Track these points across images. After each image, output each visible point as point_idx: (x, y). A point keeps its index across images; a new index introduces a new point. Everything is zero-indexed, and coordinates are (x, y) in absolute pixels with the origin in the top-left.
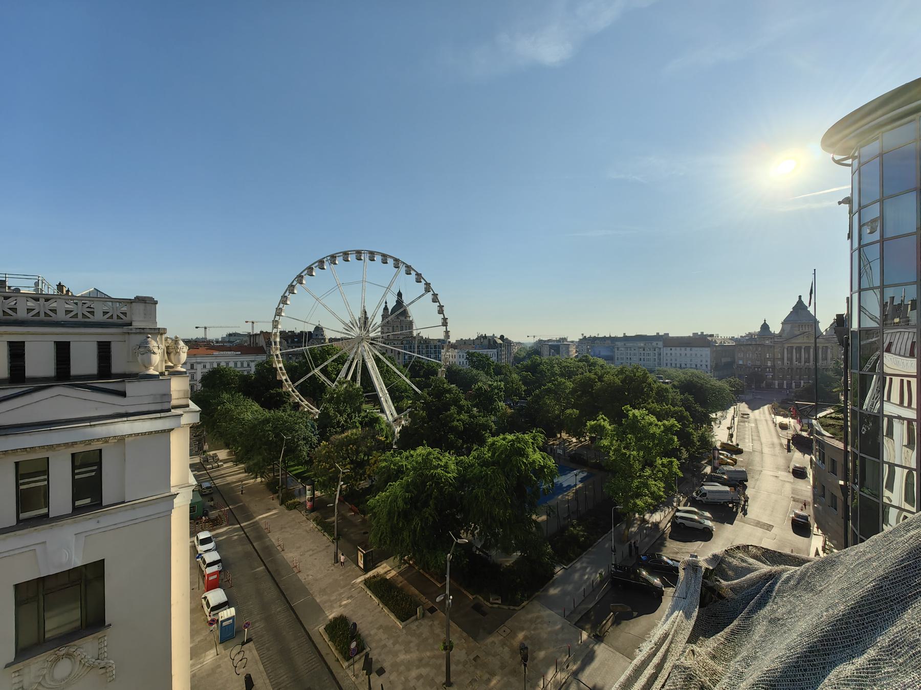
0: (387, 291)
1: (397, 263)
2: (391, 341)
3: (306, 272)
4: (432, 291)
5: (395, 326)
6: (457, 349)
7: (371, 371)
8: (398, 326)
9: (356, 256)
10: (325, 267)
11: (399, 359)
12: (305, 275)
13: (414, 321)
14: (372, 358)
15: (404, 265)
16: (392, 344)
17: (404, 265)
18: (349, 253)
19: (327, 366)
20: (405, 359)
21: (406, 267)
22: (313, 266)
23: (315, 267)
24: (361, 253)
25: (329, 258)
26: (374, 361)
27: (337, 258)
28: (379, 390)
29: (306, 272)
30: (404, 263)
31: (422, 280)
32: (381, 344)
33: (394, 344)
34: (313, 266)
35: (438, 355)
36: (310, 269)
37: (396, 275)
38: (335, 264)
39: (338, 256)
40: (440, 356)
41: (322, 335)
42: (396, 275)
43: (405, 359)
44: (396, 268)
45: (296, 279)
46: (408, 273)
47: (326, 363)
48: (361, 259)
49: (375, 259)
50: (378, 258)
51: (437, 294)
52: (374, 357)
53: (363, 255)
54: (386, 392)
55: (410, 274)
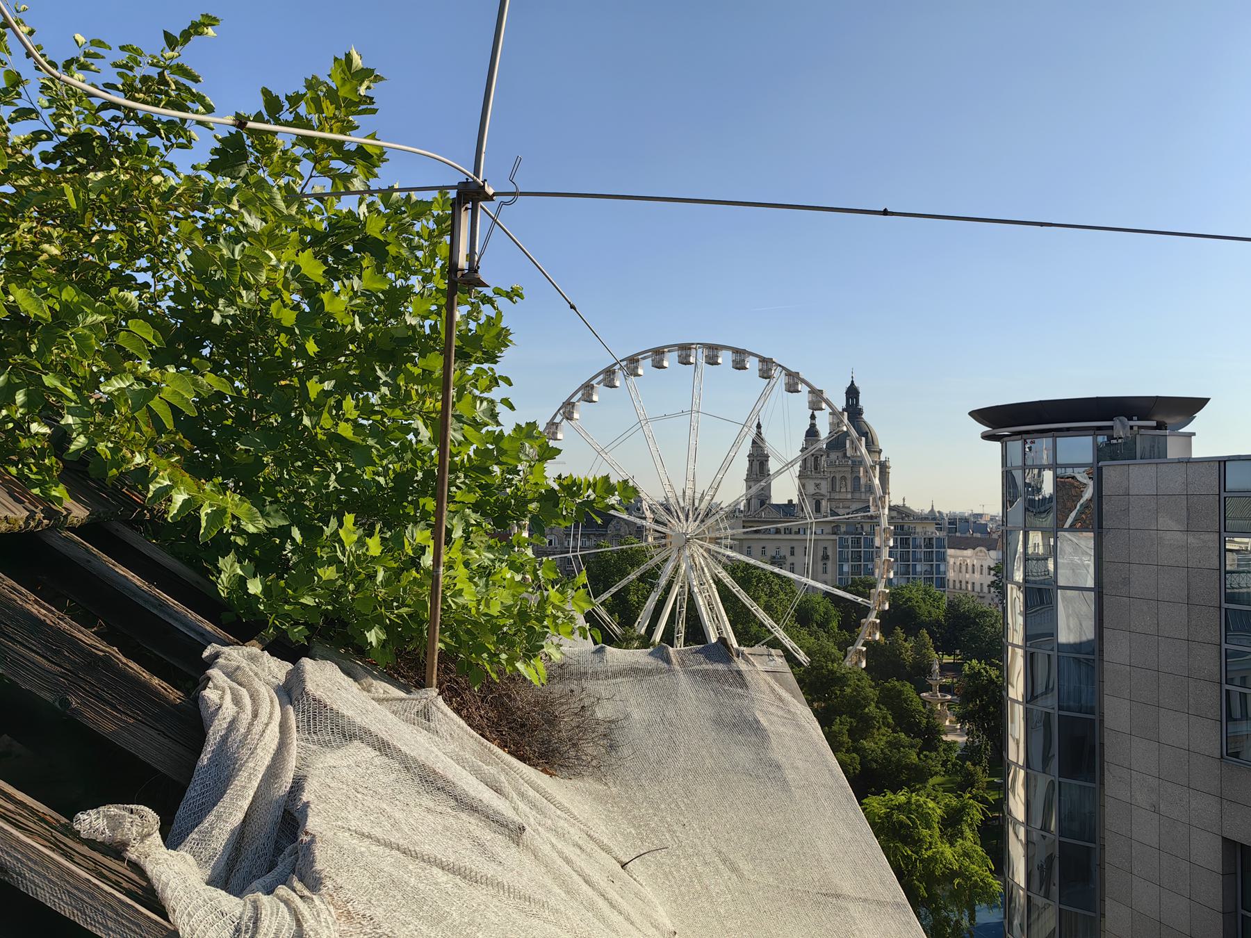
0: (743, 433)
1: (767, 367)
3: (579, 395)
5: (838, 476)
7: (703, 609)
8: (843, 478)
9: (679, 356)
10: (617, 384)
11: (825, 572)
12: (578, 401)
13: (891, 464)
14: (711, 581)
18: (666, 350)
19: (625, 589)
20: (841, 572)
21: (786, 375)
22: (594, 382)
23: (599, 383)
24: (690, 349)
25: (623, 364)
27: (642, 362)
29: (579, 395)
30: (784, 368)
31: (824, 405)
34: (594, 382)
35: (938, 566)
36: (588, 389)
37: (764, 395)
38: (637, 375)
39: (643, 359)
40: (942, 568)
41: (638, 509)
42: (764, 395)
43: (841, 572)
44: (766, 378)
45: (561, 411)
46: (792, 389)
47: (624, 582)
48: (689, 363)
49: (720, 361)
50: (725, 358)
52: (714, 580)
53: (693, 351)
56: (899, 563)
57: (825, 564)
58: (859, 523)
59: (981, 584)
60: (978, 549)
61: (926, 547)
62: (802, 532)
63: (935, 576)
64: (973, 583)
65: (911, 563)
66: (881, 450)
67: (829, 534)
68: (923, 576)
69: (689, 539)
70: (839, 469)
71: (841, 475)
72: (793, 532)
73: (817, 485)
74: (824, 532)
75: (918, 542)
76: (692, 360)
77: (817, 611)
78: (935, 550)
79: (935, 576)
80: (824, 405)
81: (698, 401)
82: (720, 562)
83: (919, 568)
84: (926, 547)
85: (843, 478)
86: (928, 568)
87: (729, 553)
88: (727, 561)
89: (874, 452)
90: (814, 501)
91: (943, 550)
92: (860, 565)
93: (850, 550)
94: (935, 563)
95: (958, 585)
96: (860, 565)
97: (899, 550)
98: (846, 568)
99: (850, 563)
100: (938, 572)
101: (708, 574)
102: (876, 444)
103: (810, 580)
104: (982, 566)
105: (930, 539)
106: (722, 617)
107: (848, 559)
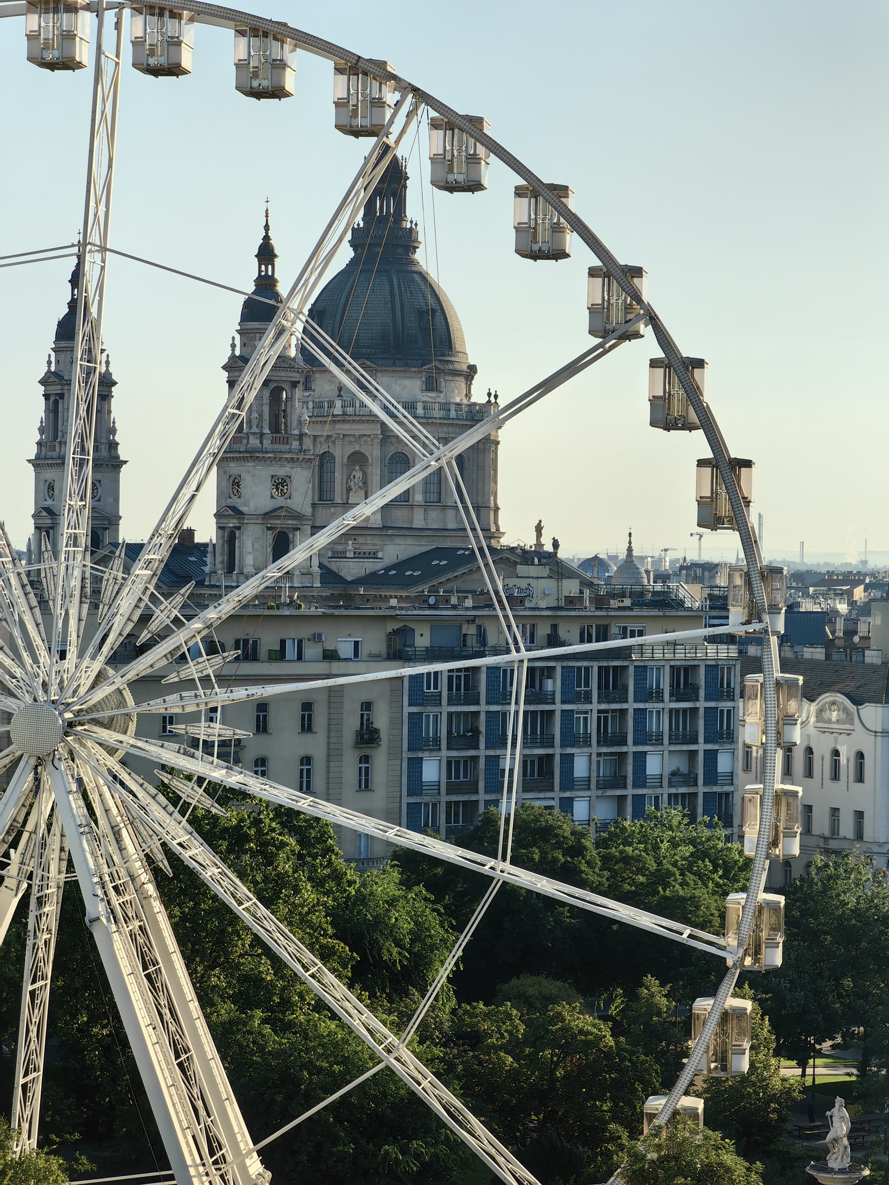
2: (304, 632)
4: (647, 331)
5: (341, 453)
6: (875, 700)
7: (130, 981)
11: (365, 783)
14: (144, 876)
15: (426, 113)
16: (312, 651)
17: (426, 113)
20: (415, 784)
26: (157, 906)
28: (190, 1154)
31: (573, 242)
32: (221, 696)
33: (330, 656)
35: (711, 757)
40: (723, 764)
43: (415, 784)
44: (357, 133)
48: (69, 64)
51: (700, 363)
52: (157, 872)
54: (255, 1166)
55: (475, 186)
56: (595, 749)
57: (365, 759)
58: (472, 620)
59: (835, 811)
60: (827, 698)
61: (677, 695)
62: (291, 652)
63: (701, 789)
64: (860, 815)
65: (630, 748)
66: (473, 369)
67: (375, 658)
68: (666, 791)
69: (71, 724)
71: (349, 450)
72: (263, 652)
73: (280, 484)
74: (364, 651)
75: (652, 680)
76: (84, 53)
77: (392, 933)
78: (702, 704)
79: (701, 789)
80: (573, 242)
81: (102, 208)
82: (175, 799)
83: (653, 766)
84: (677, 695)
85: (358, 459)
86: (681, 764)
87: (218, 773)
88: (208, 802)
89: (457, 373)
90: (270, 536)
91: (726, 705)
92: (475, 759)
93: (446, 709)
94: (701, 747)
95: (847, 828)
96: (475, 759)
97: (595, 706)
98: (431, 771)
99: (445, 753)
100: (712, 776)
101: (131, 849)
102: (458, 347)
103: (507, 866)
104: (836, 753)
105: (689, 670)
106: (185, 1003)
107: (437, 741)
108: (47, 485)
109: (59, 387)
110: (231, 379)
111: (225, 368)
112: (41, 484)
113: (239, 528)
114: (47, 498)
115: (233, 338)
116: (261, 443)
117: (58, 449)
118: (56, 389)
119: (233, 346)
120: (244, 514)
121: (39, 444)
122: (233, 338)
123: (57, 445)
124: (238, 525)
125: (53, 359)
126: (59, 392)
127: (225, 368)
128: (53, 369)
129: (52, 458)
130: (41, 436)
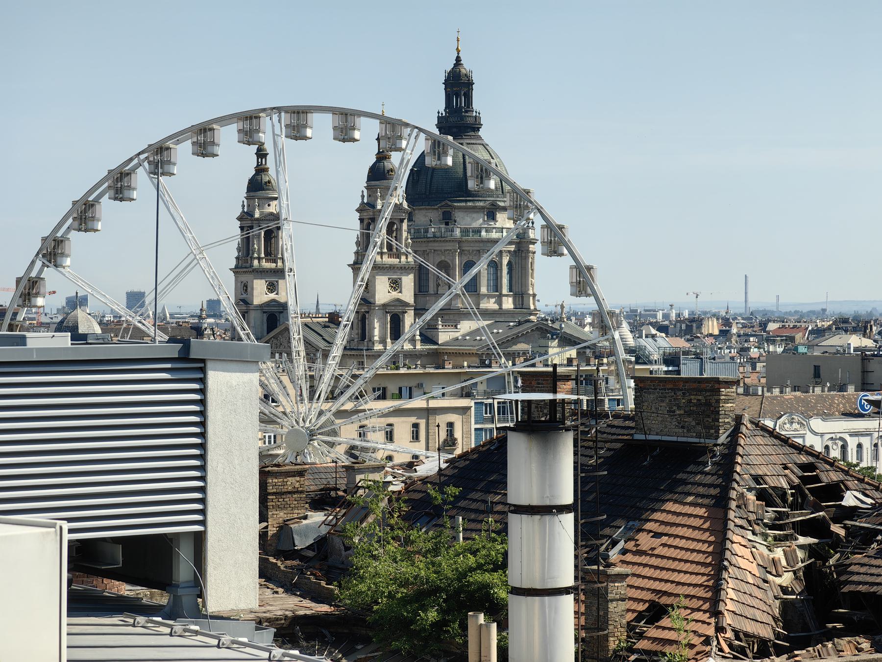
70: (436, 246)
108: (243, 285)
109: (250, 222)
110: (362, 217)
111: (357, 210)
112: (239, 284)
113: (368, 312)
114: (243, 293)
115: (363, 191)
116: (382, 258)
117: (249, 262)
118: (247, 223)
119: (363, 196)
120: (371, 303)
121: (237, 258)
122: (363, 191)
123: (249, 259)
124: (367, 310)
125: (245, 204)
126: (250, 225)
127: (357, 210)
128: (246, 210)
129: (246, 268)
130: (239, 253)
